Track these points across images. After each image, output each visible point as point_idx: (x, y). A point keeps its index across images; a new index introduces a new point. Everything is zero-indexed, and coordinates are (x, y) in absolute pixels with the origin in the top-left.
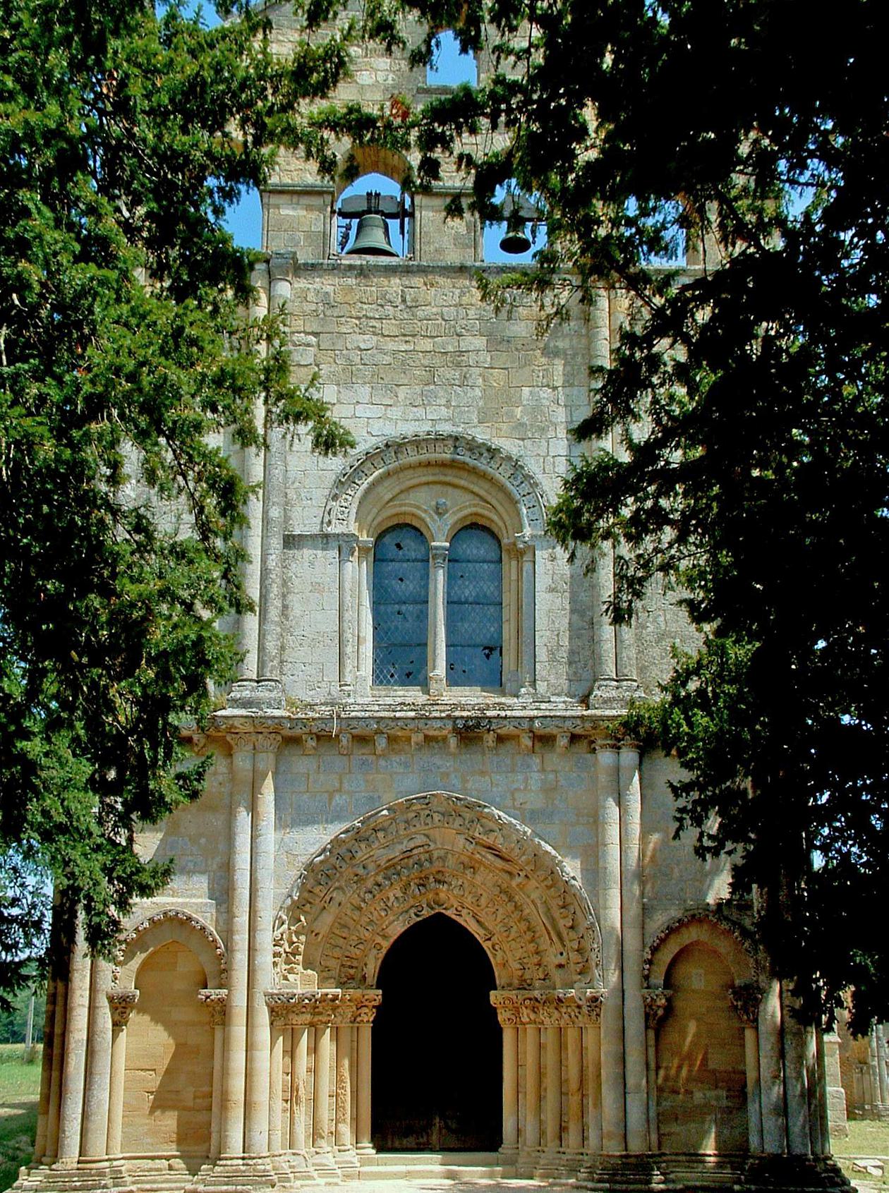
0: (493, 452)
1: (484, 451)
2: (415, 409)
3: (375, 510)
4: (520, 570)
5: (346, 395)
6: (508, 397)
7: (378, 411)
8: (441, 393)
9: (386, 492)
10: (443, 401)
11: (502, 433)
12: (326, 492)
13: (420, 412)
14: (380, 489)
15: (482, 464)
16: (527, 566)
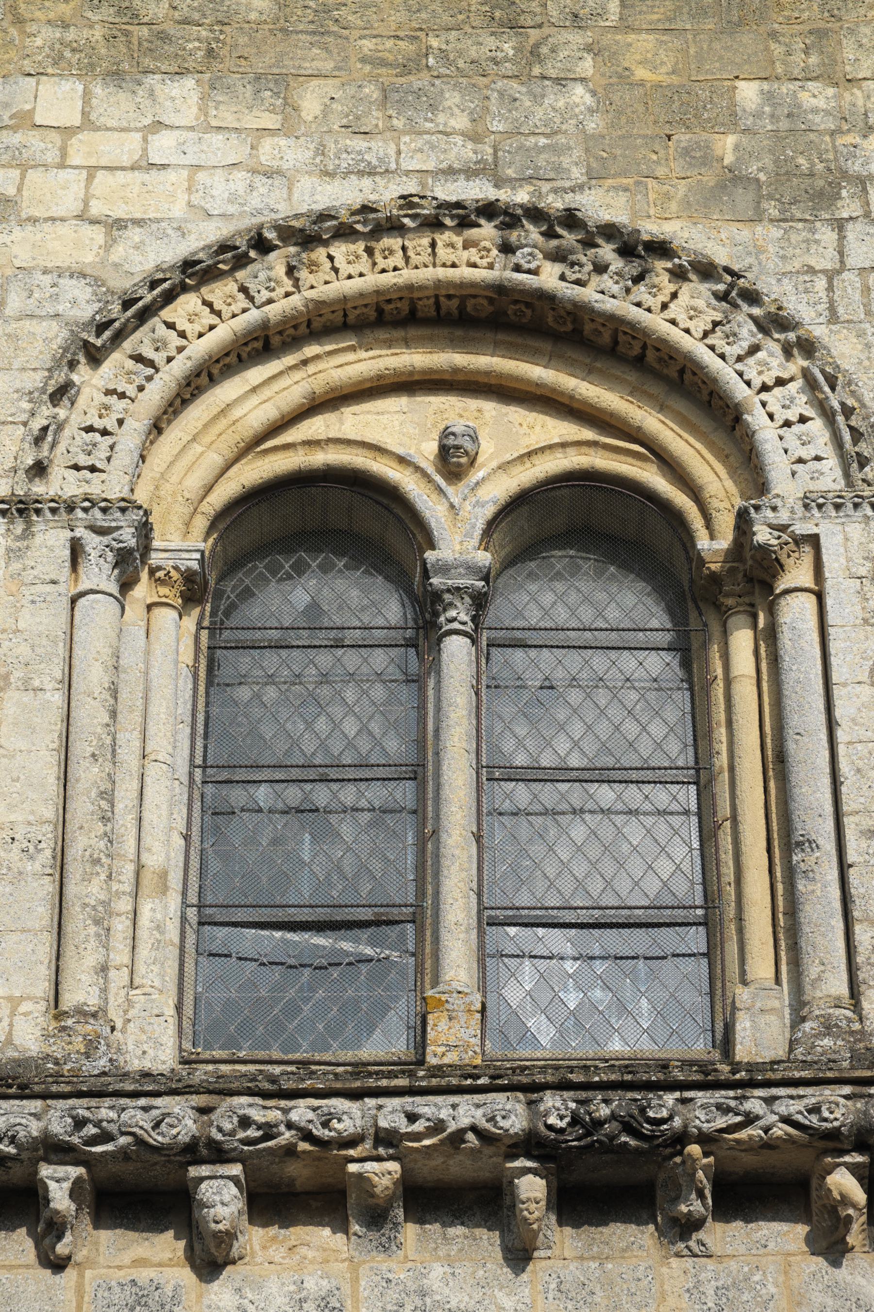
0: (641, 252)
1: (607, 252)
2: (358, 143)
3: (215, 459)
4: (770, 638)
5: (113, 104)
6: (687, 109)
7: (222, 149)
8: (452, 98)
9: (256, 395)
10: (461, 122)
11: (674, 206)
12: (36, 380)
13: (377, 149)
14: (229, 390)
15: (604, 293)
16: (797, 614)
